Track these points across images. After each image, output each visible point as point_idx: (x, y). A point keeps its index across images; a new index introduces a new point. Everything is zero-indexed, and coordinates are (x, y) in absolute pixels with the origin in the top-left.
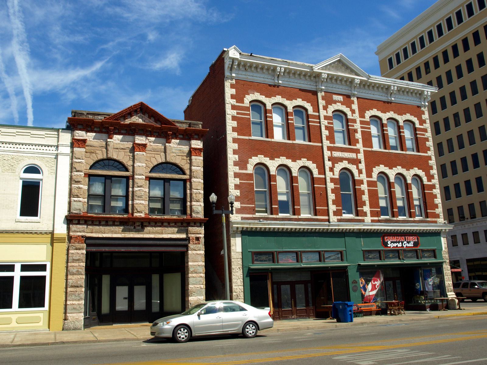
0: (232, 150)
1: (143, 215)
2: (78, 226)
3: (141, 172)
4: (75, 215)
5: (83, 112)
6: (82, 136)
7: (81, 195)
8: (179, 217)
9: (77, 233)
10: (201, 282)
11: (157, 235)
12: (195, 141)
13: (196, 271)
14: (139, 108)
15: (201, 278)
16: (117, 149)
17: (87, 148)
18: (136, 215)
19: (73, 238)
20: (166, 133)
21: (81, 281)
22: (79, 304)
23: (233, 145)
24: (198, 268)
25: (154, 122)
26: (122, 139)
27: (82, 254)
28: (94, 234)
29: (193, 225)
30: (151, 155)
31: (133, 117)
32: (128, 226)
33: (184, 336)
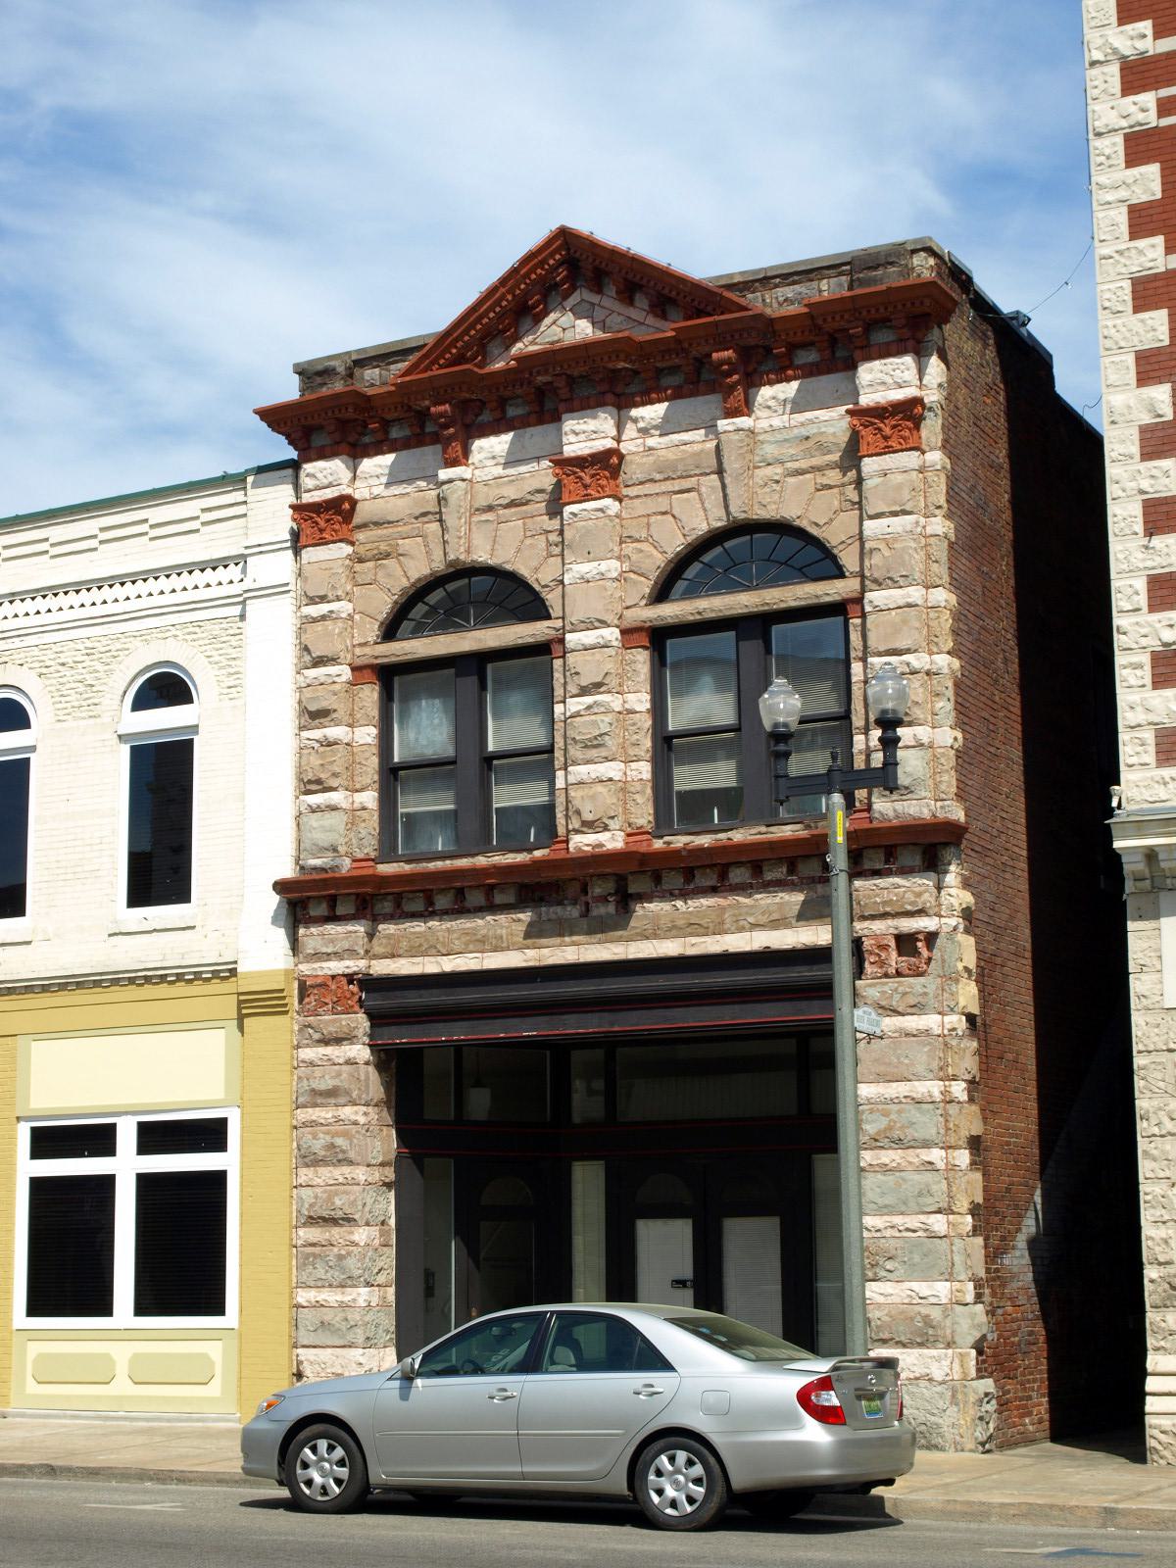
0: (1130, 360)
1: (612, 840)
2: (333, 929)
3: (597, 610)
4: (315, 876)
5: (332, 363)
6: (330, 485)
7: (335, 775)
8: (808, 827)
9: (324, 965)
10: (930, 1200)
11: (694, 940)
12: (877, 364)
13: (897, 1133)
14: (560, 264)
15: (929, 1177)
16: (490, 508)
17: (361, 536)
18: (582, 842)
19: (312, 986)
20: (703, 361)
21: (346, 1193)
22: (343, 1306)
23: (1138, 327)
24: (913, 1113)
25: (651, 320)
26: (510, 452)
27: (350, 1062)
28: (403, 961)
29: (878, 866)
30: (651, 505)
31: (547, 321)
32: (560, 903)
33: (318, 1479)
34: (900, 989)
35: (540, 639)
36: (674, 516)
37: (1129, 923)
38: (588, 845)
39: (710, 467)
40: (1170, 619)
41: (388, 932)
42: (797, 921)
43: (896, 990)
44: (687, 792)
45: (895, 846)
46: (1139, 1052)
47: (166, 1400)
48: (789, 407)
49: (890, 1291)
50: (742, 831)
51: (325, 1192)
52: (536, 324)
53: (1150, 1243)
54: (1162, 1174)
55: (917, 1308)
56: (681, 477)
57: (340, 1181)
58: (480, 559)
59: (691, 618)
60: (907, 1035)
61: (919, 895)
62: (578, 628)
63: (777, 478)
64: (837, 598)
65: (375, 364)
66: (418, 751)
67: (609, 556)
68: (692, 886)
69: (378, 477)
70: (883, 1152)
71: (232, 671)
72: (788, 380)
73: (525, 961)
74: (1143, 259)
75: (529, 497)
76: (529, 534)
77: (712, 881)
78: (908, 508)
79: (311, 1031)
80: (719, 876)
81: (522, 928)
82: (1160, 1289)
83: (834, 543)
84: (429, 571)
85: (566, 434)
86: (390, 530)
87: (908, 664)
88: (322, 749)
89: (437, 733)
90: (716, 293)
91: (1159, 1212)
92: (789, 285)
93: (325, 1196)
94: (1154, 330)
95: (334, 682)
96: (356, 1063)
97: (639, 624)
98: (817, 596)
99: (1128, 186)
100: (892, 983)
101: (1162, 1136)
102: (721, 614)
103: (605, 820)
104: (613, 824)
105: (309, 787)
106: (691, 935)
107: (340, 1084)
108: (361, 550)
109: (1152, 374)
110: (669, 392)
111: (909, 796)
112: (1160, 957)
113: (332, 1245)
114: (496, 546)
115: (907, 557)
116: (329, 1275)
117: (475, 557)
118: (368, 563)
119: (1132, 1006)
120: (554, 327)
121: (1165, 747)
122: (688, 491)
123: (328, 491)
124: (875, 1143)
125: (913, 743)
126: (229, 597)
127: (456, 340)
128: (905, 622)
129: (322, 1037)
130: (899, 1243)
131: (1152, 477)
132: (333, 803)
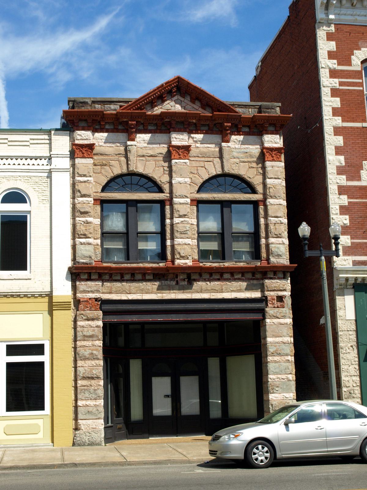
0: (334, 148)
1: (189, 263)
2: (89, 283)
3: (184, 193)
4: (83, 265)
5: (87, 100)
6: (87, 139)
7: (91, 233)
8: (248, 264)
9: (87, 294)
10: (288, 371)
11: (213, 294)
12: (270, 136)
13: (279, 352)
14: (175, 87)
15: (288, 364)
16: (143, 156)
17: (95, 157)
18: (179, 262)
19: (83, 301)
20: (221, 125)
21: (98, 369)
22: (96, 406)
23: (335, 140)
24: (283, 346)
25: (200, 109)
26: (150, 140)
27: (97, 327)
28: (113, 295)
29: (272, 276)
30: (198, 164)
31: (166, 103)
32: (167, 280)
33: (263, 458)
34: (279, 311)
35: (161, 199)
36: (205, 168)
37: (337, 297)
38: (182, 263)
39: (216, 156)
40: (345, 218)
41: (107, 285)
42: (245, 290)
43: (278, 311)
44: (204, 250)
45: (276, 271)
46: (340, 331)
47: (13, 440)
48: (240, 143)
49: (278, 396)
50: (228, 263)
51: (89, 369)
52: (162, 103)
53: (344, 381)
54: (347, 363)
55: (285, 401)
56: (208, 157)
57: (94, 365)
58: (140, 171)
59: (211, 199)
60: (281, 324)
61: (284, 285)
62: (178, 197)
63: (237, 162)
64: (256, 199)
65: (99, 103)
66: (112, 228)
67: (188, 177)
68: (212, 278)
69: (101, 139)
70: (275, 357)
71: (44, 194)
72: (240, 135)
73: (158, 297)
74: (336, 122)
75: (157, 155)
76: (157, 166)
77: (218, 277)
78: (279, 177)
79: (82, 316)
80: (220, 275)
81: (156, 287)
82: (347, 394)
83: (255, 184)
84: (121, 172)
85: (173, 138)
86: (106, 157)
87: (280, 221)
88: (85, 224)
89: (119, 223)
90: (228, 106)
91: (346, 373)
92: (240, 108)
93: (89, 370)
94: (339, 141)
95: (89, 203)
96: (100, 327)
97: (195, 199)
98: (250, 198)
99: (332, 102)
100: (277, 310)
101: (346, 353)
102: (220, 199)
103: (188, 256)
104: (190, 258)
105: (80, 236)
106: (213, 292)
107: (95, 334)
108: (96, 162)
109: (339, 153)
110: (204, 131)
111: (281, 258)
112: (345, 306)
113: (91, 386)
114: (145, 168)
115: (280, 191)
116: (90, 396)
117: (138, 170)
118: (98, 167)
119: (338, 319)
120: (168, 105)
121: (344, 251)
122: (210, 162)
123: (85, 141)
124: (273, 354)
125: (282, 243)
126: (43, 170)
127: (140, 102)
128: (279, 209)
129: (87, 318)
130: (280, 383)
131: (340, 179)
132: (90, 242)
